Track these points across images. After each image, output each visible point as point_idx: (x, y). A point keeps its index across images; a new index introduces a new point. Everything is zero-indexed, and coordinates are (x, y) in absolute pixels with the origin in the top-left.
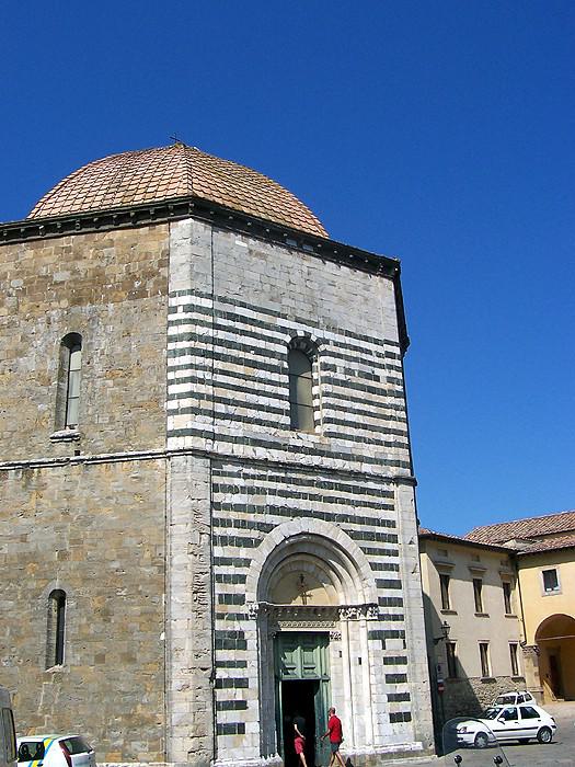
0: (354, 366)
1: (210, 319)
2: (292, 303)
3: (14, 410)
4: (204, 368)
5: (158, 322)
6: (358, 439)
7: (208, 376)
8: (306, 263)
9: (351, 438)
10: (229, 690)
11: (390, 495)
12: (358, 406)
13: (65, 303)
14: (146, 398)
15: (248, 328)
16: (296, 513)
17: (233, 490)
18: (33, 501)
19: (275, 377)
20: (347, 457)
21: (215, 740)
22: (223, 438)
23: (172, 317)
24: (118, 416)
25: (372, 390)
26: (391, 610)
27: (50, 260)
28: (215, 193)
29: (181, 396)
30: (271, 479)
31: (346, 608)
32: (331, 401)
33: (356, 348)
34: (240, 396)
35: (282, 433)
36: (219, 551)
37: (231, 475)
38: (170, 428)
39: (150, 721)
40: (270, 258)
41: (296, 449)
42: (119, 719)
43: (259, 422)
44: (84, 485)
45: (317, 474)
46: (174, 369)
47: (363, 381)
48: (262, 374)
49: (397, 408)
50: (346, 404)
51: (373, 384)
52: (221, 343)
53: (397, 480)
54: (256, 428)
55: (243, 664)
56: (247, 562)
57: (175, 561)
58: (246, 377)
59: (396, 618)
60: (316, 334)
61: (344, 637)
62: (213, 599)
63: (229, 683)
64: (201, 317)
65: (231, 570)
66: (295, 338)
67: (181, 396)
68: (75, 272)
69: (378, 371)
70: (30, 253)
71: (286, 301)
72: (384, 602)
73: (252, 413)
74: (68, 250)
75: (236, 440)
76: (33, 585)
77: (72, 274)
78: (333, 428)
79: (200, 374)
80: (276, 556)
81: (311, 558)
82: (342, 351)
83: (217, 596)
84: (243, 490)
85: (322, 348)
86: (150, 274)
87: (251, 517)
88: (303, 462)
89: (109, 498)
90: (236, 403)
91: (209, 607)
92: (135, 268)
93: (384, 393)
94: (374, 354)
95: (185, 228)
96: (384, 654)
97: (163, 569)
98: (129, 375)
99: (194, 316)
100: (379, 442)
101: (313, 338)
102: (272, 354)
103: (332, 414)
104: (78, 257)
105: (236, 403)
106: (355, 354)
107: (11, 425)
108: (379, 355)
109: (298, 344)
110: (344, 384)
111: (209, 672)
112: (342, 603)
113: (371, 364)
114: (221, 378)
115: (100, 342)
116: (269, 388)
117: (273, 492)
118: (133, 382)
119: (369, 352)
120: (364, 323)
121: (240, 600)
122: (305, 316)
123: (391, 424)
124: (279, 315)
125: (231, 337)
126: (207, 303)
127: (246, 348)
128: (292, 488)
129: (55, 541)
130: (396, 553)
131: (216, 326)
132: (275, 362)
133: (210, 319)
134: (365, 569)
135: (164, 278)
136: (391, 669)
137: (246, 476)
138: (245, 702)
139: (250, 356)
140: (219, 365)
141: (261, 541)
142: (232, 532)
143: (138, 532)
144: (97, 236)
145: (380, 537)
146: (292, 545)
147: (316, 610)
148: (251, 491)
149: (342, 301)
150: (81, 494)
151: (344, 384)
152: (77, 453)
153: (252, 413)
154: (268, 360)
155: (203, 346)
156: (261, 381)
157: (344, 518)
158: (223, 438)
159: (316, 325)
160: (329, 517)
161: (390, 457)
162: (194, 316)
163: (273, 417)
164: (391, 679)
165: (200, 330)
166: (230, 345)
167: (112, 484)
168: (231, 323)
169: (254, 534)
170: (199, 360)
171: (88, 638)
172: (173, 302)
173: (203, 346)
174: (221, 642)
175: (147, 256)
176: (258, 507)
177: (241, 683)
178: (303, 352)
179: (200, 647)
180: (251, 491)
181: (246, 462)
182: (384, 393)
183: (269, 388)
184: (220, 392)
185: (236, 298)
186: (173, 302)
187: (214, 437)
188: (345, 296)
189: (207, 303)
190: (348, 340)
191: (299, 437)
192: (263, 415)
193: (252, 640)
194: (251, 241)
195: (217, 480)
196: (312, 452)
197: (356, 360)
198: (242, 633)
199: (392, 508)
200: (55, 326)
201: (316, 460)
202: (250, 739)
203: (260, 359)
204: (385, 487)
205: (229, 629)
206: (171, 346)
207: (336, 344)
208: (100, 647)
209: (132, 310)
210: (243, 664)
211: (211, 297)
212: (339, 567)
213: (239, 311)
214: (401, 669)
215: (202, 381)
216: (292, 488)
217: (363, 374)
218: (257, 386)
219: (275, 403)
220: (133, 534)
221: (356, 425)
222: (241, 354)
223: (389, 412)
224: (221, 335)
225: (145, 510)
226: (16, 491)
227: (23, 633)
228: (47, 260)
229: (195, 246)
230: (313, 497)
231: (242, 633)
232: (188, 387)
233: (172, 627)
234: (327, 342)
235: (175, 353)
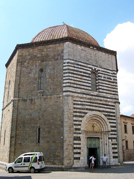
0: (106, 76)
1: (73, 65)
2: (91, 61)
3: (29, 86)
4: (72, 77)
5: (61, 66)
6: (107, 93)
7: (73, 78)
8: (95, 52)
9: (105, 93)
12: (106, 85)
13: (40, 62)
14: (58, 83)
15: (82, 67)
16: (92, 110)
17: (78, 104)
18: (33, 107)
20: (104, 97)
21: (73, 161)
23: (64, 65)
24: (52, 87)
25: (110, 82)
26: (114, 133)
27: (36, 52)
28: (73, 36)
29: (66, 83)
33: (106, 72)
34: (80, 83)
35: (89, 92)
36: (75, 118)
38: (64, 90)
39: (59, 156)
40: (86, 51)
41: (92, 95)
42: (52, 155)
43: (84, 89)
44: (44, 103)
46: (65, 77)
47: (108, 80)
48: (85, 78)
50: (104, 85)
51: (110, 80)
54: (83, 90)
55: (80, 144)
56: (81, 121)
57: (65, 120)
59: (115, 134)
60: (97, 69)
62: (73, 129)
63: (77, 148)
65: (77, 123)
67: (66, 83)
68: (42, 54)
69: (111, 78)
70: (32, 50)
71: (90, 61)
72: (112, 131)
73: (83, 87)
74: (40, 49)
75: (79, 93)
76: (33, 125)
77: (41, 55)
78: (101, 90)
79: (71, 78)
84: (80, 104)
85: (98, 72)
86: (59, 55)
87: (82, 111)
89: (50, 106)
90: (79, 85)
92: (56, 53)
94: (110, 73)
95: (67, 44)
96: (112, 143)
97: (62, 122)
98: (54, 78)
99: (69, 64)
100: (111, 94)
101: (96, 70)
102: (87, 73)
104: (43, 51)
105: (79, 85)
106: (106, 73)
107: (28, 89)
108: (111, 74)
109: (93, 71)
110: (104, 80)
113: (110, 76)
114: (75, 79)
115: (48, 71)
116: (86, 81)
117: (87, 105)
118: (55, 80)
119: (109, 73)
120: (108, 66)
121: (79, 129)
122: (95, 65)
125: (78, 69)
126: (72, 62)
127: (81, 72)
128: (92, 104)
129: (38, 116)
130: (115, 120)
131: (74, 67)
132: (88, 75)
133: (73, 65)
134: (108, 123)
135: (62, 56)
136: (113, 146)
137: (81, 101)
138: (80, 152)
139: (82, 74)
140: (75, 76)
141: (84, 116)
142: (78, 114)
143: (57, 114)
144: (47, 46)
145: (111, 116)
146: (91, 117)
148: (82, 105)
149: (103, 61)
150: (44, 105)
151: (104, 80)
152: (43, 96)
153: (83, 87)
154: (86, 75)
155: (71, 71)
156: (84, 79)
159: (97, 67)
160: (100, 111)
161: (114, 97)
162: (69, 64)
163: (87, 88)
164: (113, 148)
165: (71, 68)
166: (77, 71)
167: (51, 103)
168: (78, 66)
169: (83, 115)
170: (70, 75)
171: (45, 137)
172: (64, 61)
173: (71, 71)
174: (76, 139)
175: (58, 51)
176: (84, 108)
177: (79, 148)
178: (94, 73)
179: (70, 140)
180: (82, 105)
183: (86, 81)
184: (76, 82)
186: (64, 61)
188: (104, 60)
189: (72, 62)
190: (104, 70)
191: (93, 93)
192: (85, 87)
197: (106, 75)
198: (80, 137)
199: (114, 109)
200: (38, 67)
201: (97, 98)
203: (84, 74)
205: (77, 136)
206: (64, 71)
207: (102, 71)
208: (48, 139)
209: (55, 63)
210: (80, 144)
211: (73, 60)
213: (79, 63)
214: (116, 146)
215: (71, 80)
217: (108, 78)
218: (84, 81)
219: (88, 85)
220: (55, 114)
222: (80, 73)
224: (75, 69)
225: (58, 109)
226: (29, 104)
227: (31, 136)
228: (35, 52)
229: (69, 48)
230: (96, 106)
231: (80, 137)
233: (64, 135)
234: (100, 70)
235: (65, 73)
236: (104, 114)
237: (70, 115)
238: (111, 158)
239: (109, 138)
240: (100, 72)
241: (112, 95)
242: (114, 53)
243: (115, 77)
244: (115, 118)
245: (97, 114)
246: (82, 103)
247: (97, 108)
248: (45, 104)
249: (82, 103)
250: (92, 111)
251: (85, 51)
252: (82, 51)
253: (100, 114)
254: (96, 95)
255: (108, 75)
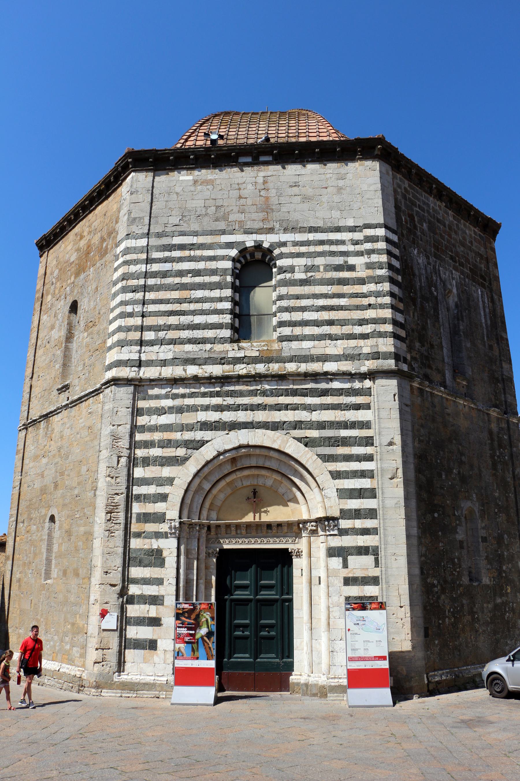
0: (320, 261)
2: (242, 217)
10: (142, 606)
11: (368, 392)
12: (321, 302)
16: (234, 426)
17: (161, 411)
19: (216, 293)
22: (150, 363)
26: (359, 524)
29: (114, 333)
30: (204, 395)
31: (305, 522)
32: (284, 303)
33: (322, 243)
34: (173, 320)
35: (218, 347)
37: (157, 397)
38: (107, 363)
40: (218, 182)
45: (261, 382)
48: (199, 294)
49: (378, 294)
50: (304, 303)
52: (155, 275)
53: (372, 375)
54: (188, 347)
55: (159, 582)
56: (170, 481)
58: (179, 301)
59: (365, 532)
60: (267, 240)
61: (305, 554)
64: (134, 256)
65: (151, 490)
66: (243, 251)
67: (114, 333)
69: (352, 260)
72: (346, 514)
75: (164, 363)
78: (287, 331)
79: (129, 309)
80: (210, 473)
81: (263, 472)
82: (303, 249)
83: (134, 516)
84: (171, 410)
85: (276, 252)
87: (177, 436)
88: (243, 372)
89: (78, 434)
90: (169, 328)
91: (122, 526)
93: (362, 281)
96: (346, 573)
99: (128, 257)
102: (214, 272)
103: (285, 316)
105: (169, 328)
106: (320, 249)
109: (252, 255)
110: (303, 283)
111: (118, 588)
112: (305, 517)
114: (152, 308)
117: (206, 408)
118: (95, 329)
119: (342, 242)
120: (336, 214)
121: (160, 518)
122: (257, 225)
123: (370, 314)
124: (224, 232)
125: (167, 266)
127: (181, 274)
128: (230, 401)
130: (369, 458)
132: (216, 279)
134: (324, 479)
136: (354, 591)
137: (175, 397)
142: (156, 452)
145: (345, 442)
146: (233, 460)
147: (269, 526)
148: (180, 410)
149: (306, 199)
151: (303, 283)
153: (185, 334)
154: (207, 279)
157: (297, 425)
158: (150, 363)
159: (271, 230)
160: (275, 426)
161: (366, 350)
162: (128, 257)
163: (210, 334)
165: (133, 269)
168: (167, 254)
169: (181, 452)
170: (129, 296)
176: (187, 425)
180: (180, 410)
181: (175, 382)
182: (362, 281)
185: (174, 229)
187: (140, 364)
188: (309, 192)
190: (311, 237)
193: (171, 560)
194: (196, 173)
195: (141, 404)
196: (255, 360)
198: (159, 552)
202: (162, 656)
203: (198, 280)
204: (357, 385)
205: (146, 547)
210: (159, 582)
212: (297, 480)
213: (178, 240)
214: (370, 590)
215: (131, 315)
216: (230, 401)
217: (329, 268)
218: (193, 307)
219: (213, 319)
221: (317, 323)
222: (177, 280)
223: (365, 301)
229: (133, 196)
231: (159, 552)
232: (119, 322)
234: (284, 244)
236: (294, 438)
237: (115, 459)
238: (337, 649)
239: (332, 552)
240: (284, 250)
241: (353, 343)
242: (374, 148)
243: (372, 256)
244: (369, 450)
245: (259, 443)
246: (178, 402)
247: (260, 416)
248: (69, 430)
249: (178, 402)
250: (232, 433)
251: (211, 182)
252: (192, 188)
253: (274, 441)
254: (257, 354)
255: (333, 254)
